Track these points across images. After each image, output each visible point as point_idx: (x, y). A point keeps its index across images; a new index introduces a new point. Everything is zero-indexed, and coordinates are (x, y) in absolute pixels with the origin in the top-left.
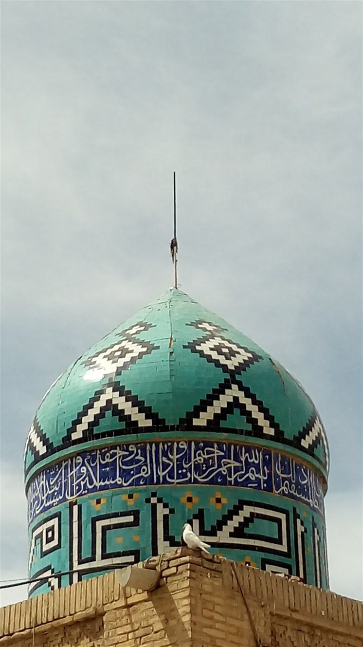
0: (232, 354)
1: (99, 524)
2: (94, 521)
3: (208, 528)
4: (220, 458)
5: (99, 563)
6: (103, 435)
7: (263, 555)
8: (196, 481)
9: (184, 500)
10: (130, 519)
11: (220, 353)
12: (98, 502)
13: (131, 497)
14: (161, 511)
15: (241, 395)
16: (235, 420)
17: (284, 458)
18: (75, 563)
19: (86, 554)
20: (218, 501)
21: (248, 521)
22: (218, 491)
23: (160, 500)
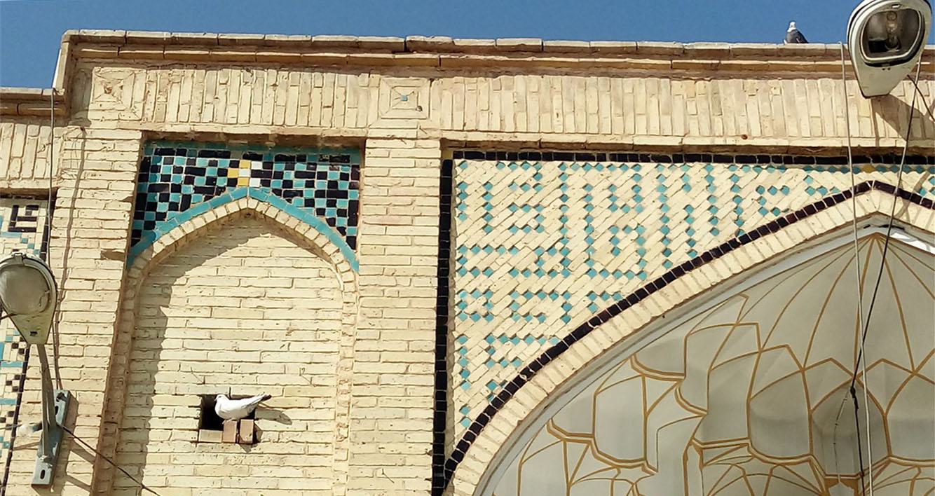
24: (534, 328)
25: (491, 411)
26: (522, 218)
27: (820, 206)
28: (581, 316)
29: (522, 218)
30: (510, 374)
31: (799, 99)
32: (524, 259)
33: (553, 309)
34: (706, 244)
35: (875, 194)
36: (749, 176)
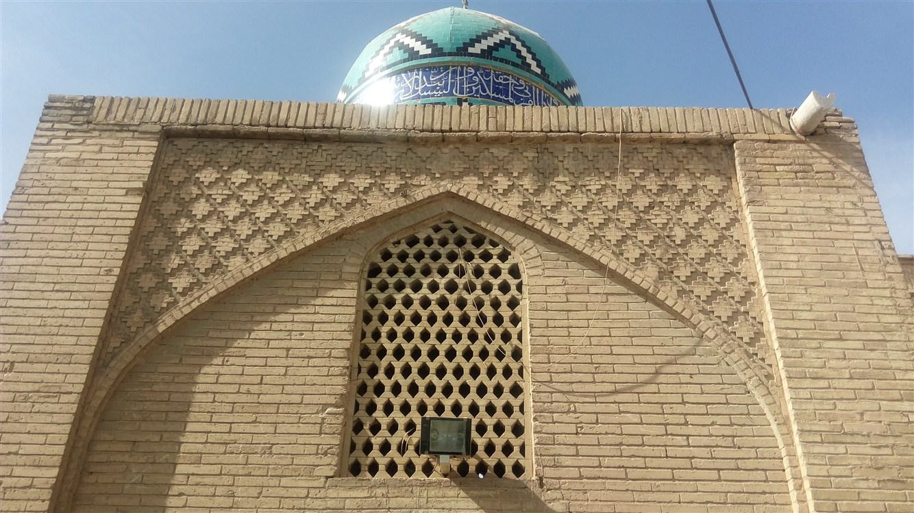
6: (502, 60)
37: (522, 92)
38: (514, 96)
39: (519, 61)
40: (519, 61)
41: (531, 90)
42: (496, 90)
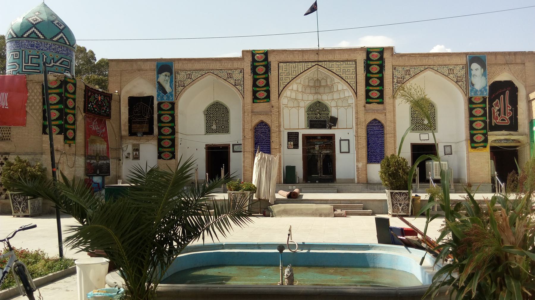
0: (61, 26)
1: (30, 57)
2: (29, 55)
3: (55, 62)
4: (58, 48)
5: (30, 64)
6: (32, 38)
7: (65, 69)
8: (53, 52)
9: (50, 55)
10: (38, 57)
11: (59, 25)
12: (30, 52)
13: (38, 52)
14: (45, 57)
15: (63, 35)
16: (62, 41)
17: (70, 49)
18: (24, 63)
19: (27, 62)
20: (57, 57)
21: (63, 61)
22: (57, 55)
23: (45, 54)
24: (287, 81)
25: (283, 89)
26: (286, 69)
27: (312, 67)
28: (290, 80)
29: (286, 69)
30: (284, 86)
31: (311, 55)
32: (286, 74)
33: (288, 79)
34: (302, 71)
35: (317, 65)
36: (306, 64)
37: (38, 45)
38: (36, 47)
39: (37, 37)
40: (37, 37)
41: (41, 44)
42: (31, 46)
